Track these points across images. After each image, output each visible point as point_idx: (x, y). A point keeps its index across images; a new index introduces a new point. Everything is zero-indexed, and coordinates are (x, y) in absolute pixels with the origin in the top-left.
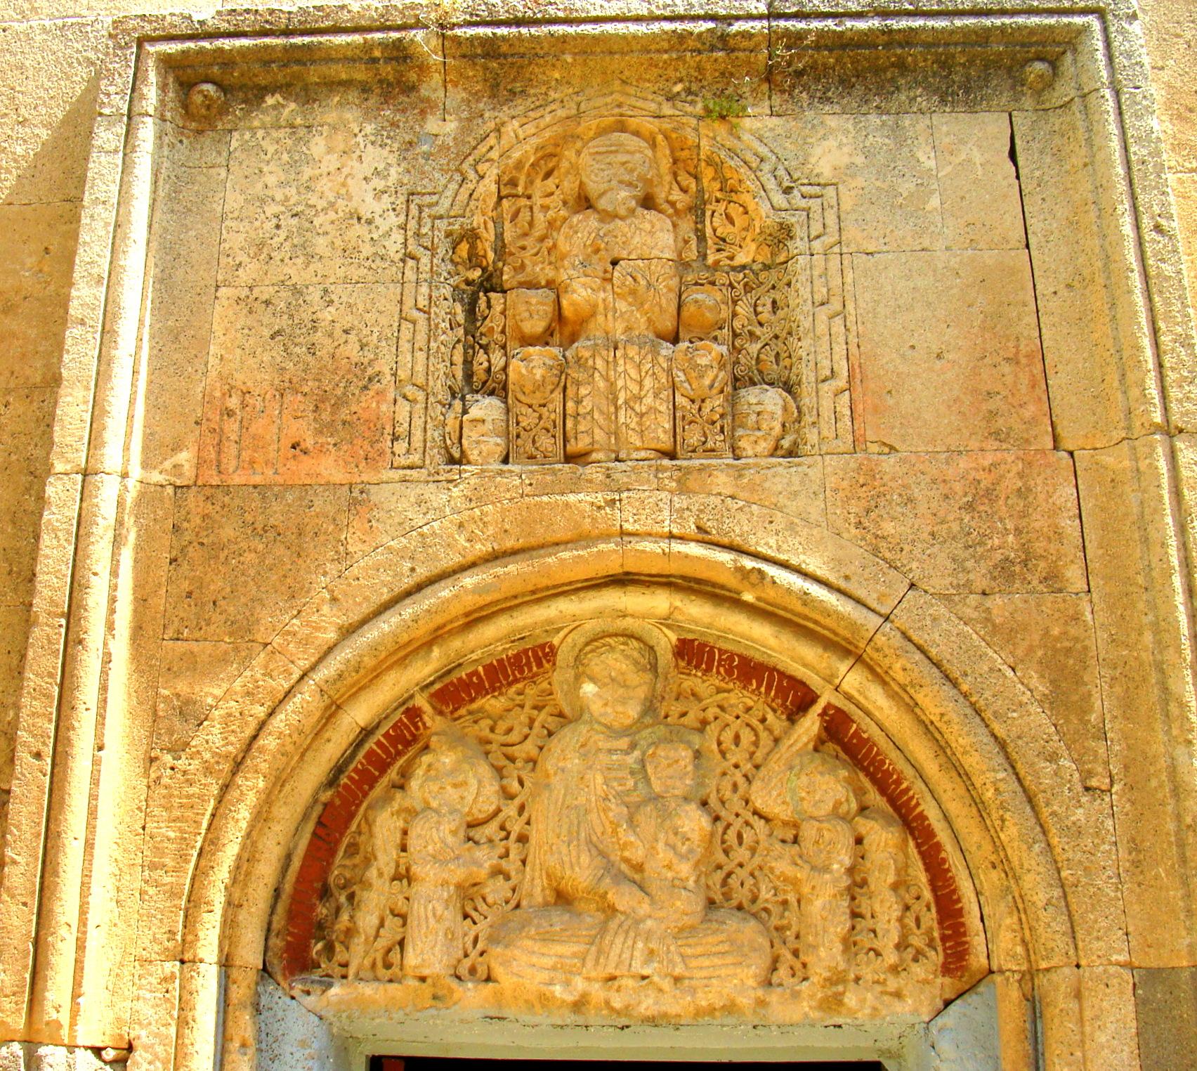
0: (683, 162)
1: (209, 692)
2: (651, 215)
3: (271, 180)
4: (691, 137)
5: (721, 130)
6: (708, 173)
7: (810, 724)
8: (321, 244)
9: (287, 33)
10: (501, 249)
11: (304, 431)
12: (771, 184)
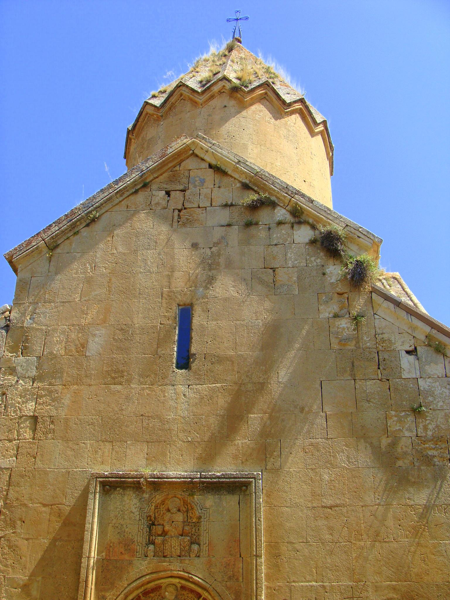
0: (185, 503)
1: (107, 594)
2: (179, 513)
3: (118, 504)
4: (186, 499)
5: (191, 498)
6: (189, 505)
8: (126, 517)
9: (121, 478)
10: (155, 518)
12: (199, 508)
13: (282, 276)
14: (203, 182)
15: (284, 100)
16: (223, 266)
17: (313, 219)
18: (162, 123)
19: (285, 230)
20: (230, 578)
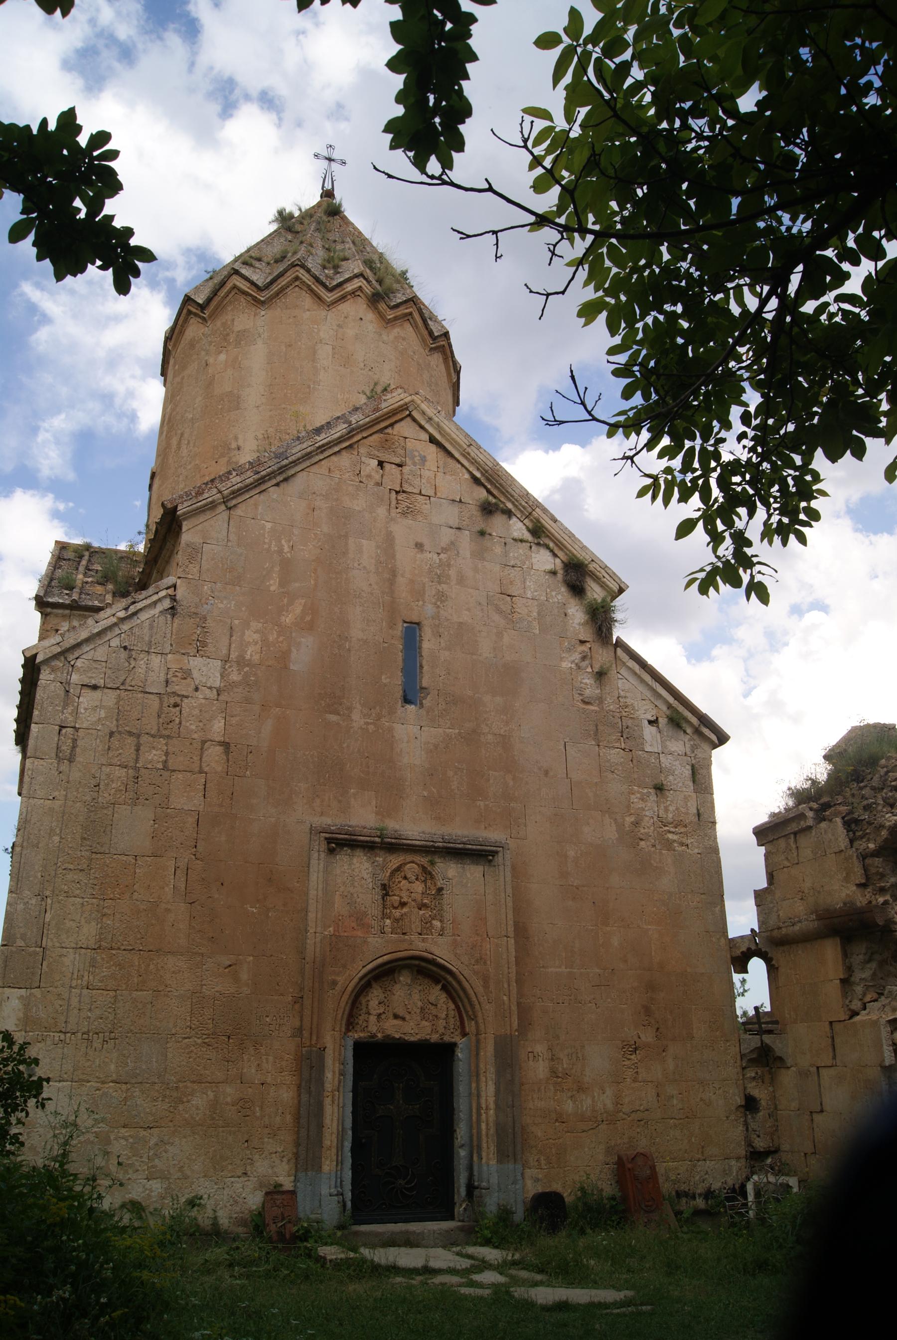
7: (440, 986)
11: (354, 924)
13: (521, 607)
14: (424, 459)
18: (263, 313)
19: (522, 549)
20: (477, 961)
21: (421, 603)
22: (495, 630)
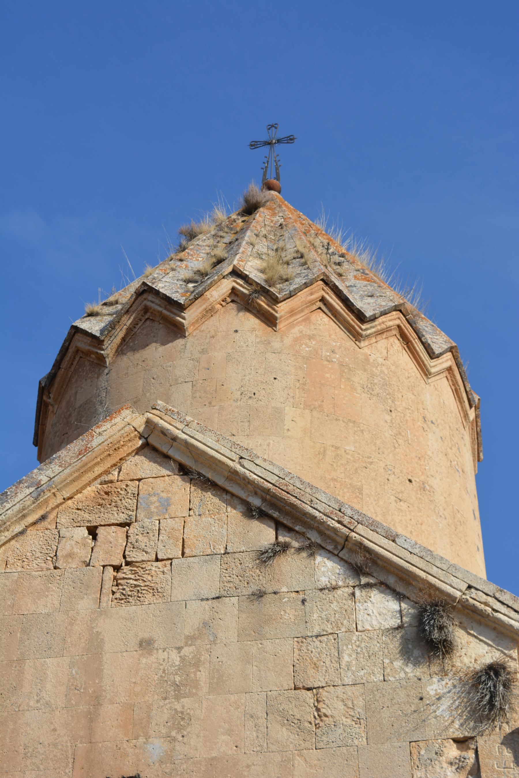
13: (334, 706)
14: (166, 504)
15: (359, 311)
16: (205, 689)
17: (397, 575)
21: (142, 740)
22: (278, 758)
